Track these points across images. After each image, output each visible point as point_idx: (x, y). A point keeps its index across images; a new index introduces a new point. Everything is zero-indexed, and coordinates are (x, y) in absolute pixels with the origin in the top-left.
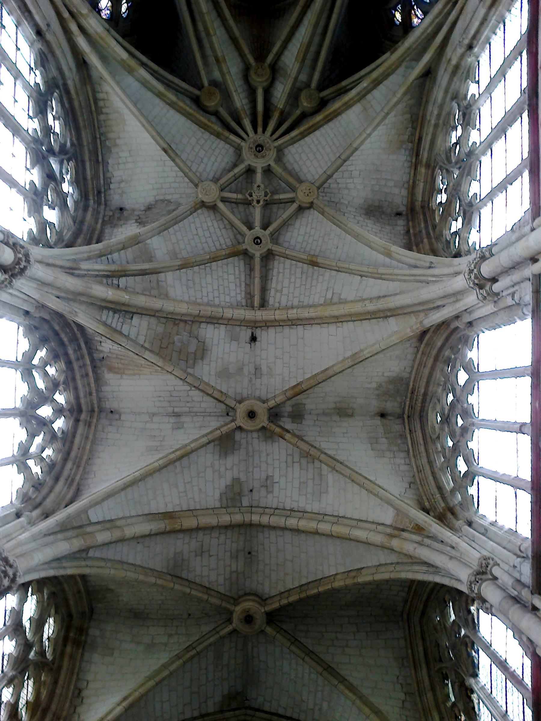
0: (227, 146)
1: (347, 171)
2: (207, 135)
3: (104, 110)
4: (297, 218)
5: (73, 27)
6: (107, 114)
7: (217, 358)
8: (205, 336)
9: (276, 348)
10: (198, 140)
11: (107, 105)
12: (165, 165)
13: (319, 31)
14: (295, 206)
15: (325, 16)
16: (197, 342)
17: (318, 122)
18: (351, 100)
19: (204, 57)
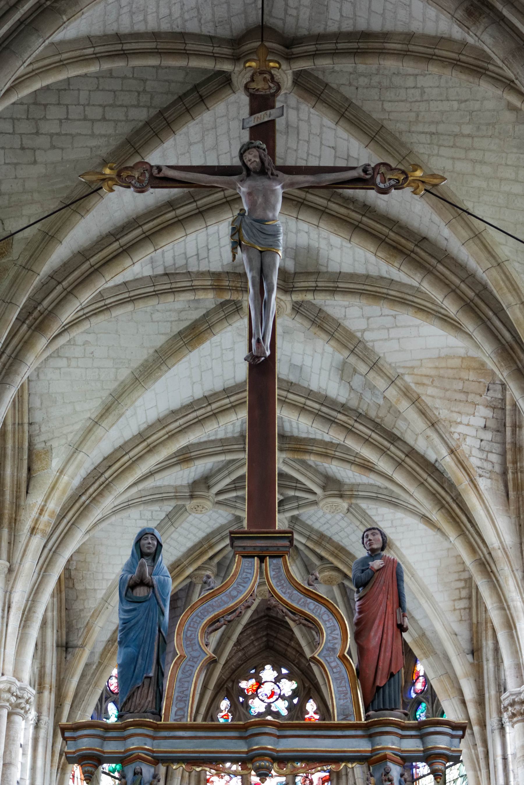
0: (309, 522)
1: (147, 520)
2: (336, 538)
3: (462, 584)
4: (211, 470)
6: (460, 580)
7: (322, 354)
8: (339, 386)
9: (233, 359)
10: (348, 536)
11: (457, 591)
12: (392, 521)
14: (215, 490)
16: (351, 383)
17: (191, 564)
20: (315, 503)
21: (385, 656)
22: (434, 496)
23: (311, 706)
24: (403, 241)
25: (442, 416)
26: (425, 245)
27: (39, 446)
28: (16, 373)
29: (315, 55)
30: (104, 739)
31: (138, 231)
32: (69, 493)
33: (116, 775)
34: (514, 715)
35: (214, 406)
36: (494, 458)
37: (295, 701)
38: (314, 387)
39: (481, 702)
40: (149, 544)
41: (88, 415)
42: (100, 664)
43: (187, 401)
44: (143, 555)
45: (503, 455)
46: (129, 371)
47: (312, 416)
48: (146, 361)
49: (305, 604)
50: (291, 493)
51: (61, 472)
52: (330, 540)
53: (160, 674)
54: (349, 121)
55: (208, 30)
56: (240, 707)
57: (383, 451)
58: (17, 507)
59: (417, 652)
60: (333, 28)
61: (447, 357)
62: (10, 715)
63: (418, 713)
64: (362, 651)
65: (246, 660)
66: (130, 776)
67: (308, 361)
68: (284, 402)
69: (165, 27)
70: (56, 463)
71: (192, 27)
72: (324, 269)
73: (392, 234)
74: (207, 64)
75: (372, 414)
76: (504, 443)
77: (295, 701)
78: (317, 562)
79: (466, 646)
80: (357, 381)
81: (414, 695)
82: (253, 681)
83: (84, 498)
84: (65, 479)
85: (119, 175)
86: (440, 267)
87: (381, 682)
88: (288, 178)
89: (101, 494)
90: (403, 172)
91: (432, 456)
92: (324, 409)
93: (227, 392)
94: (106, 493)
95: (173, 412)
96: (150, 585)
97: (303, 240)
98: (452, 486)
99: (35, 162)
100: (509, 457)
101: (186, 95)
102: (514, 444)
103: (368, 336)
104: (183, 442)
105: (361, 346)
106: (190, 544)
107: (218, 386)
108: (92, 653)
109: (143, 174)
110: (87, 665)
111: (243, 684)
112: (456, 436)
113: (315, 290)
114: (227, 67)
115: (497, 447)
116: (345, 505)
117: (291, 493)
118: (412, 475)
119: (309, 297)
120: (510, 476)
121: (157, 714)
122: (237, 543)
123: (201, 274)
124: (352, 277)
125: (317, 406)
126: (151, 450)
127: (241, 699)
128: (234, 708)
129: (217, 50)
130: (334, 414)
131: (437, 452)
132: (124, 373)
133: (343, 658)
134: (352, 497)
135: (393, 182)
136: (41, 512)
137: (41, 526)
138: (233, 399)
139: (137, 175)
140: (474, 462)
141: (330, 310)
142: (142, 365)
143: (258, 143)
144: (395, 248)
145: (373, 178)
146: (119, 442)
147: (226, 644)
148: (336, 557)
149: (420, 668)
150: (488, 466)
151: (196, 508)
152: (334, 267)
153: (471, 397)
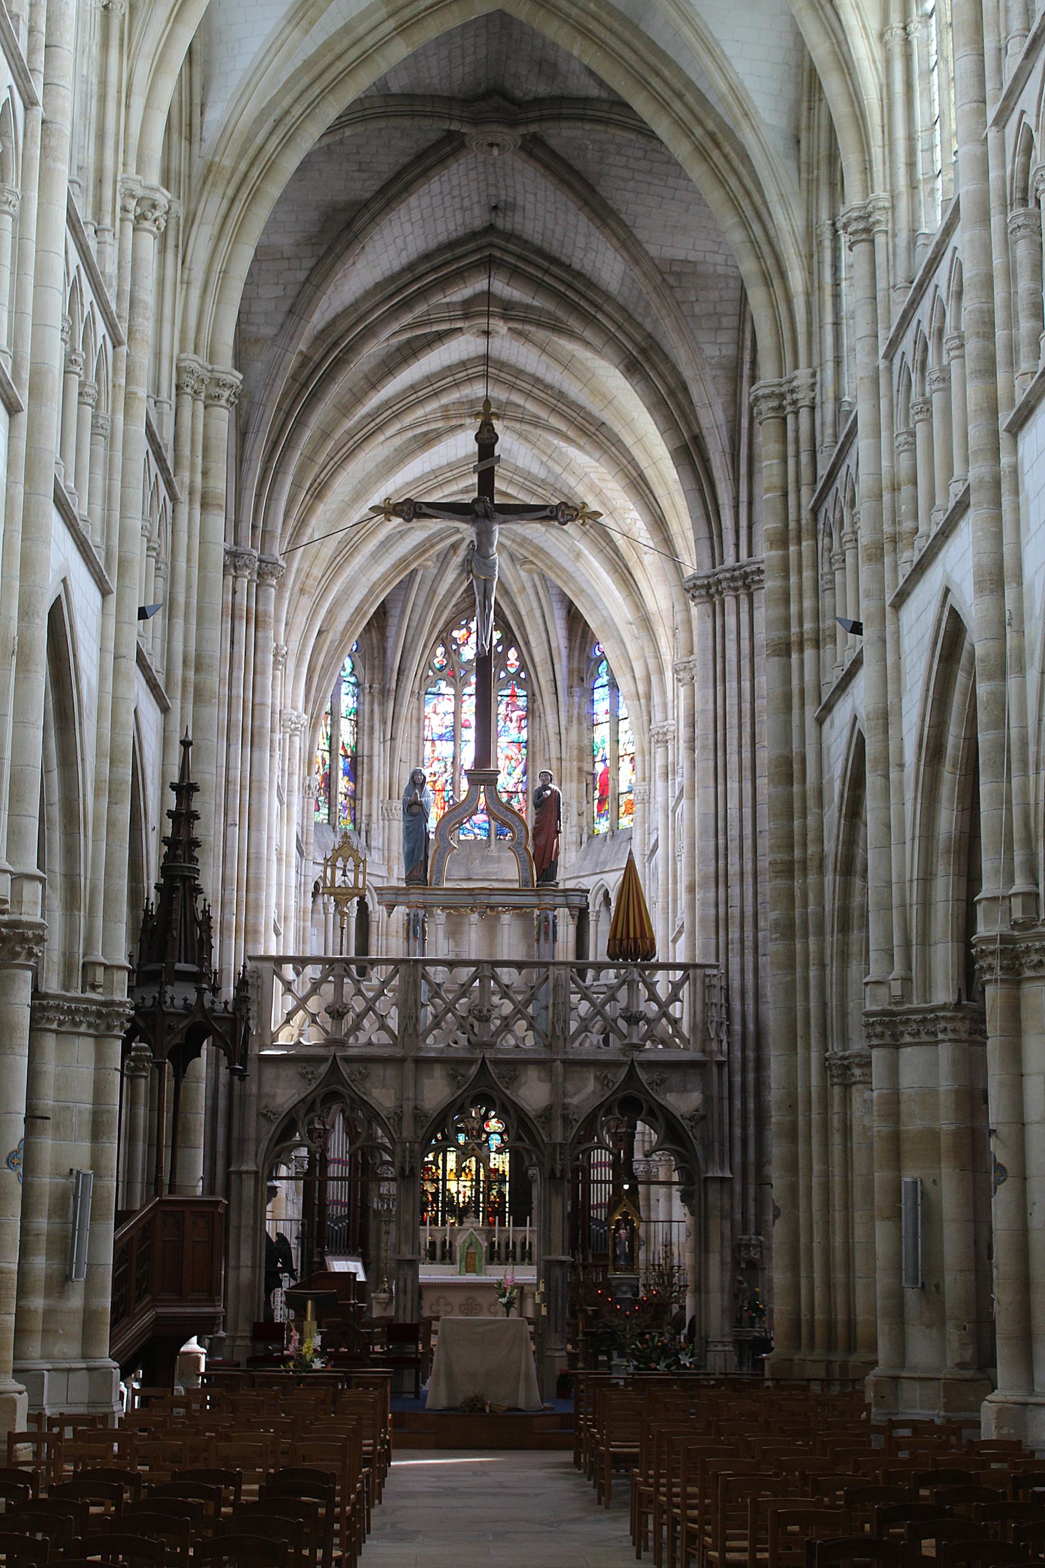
2: (535, 541)
13: (418, 610)
15: (414, 624)
17: (415, 559)
18: (383, 590)
19: (535, 586)
23: (512, 654)
24: (587, 425)
25: (618, 505)
26: (603, 429)
28: (304, 534)
33: (352, 717)
34: (658, 741)
35: (440, 478)
38: (520, 464)
41: (342, 498)
42: (341, 641)
43: (419, 475)
46: (373, 464)
47: (518, 488)
48: (388, 457)
49: (506, 816)
53: (426, 857)
56: (453, 654)
59: (599, 636)
63: (600, 669)
66: (412, 916)
73: (579, 419)
77: (500, 649)
81: (598, 653)
82: (464, 631)
83: (338, 559)
85: (394, 509)
86: (613, 449)
87: (545, 866)
89: (351, 555)
90: (576, 510)
92: (527, 483)
93: (451, 466)
94: (355, 554)
95: (407, 484)
105: (557, 451)
107: (444, 462)
109: (409, 508)
111: (456, 634)
112: (628, 521)
125: (522, 480)
127: (454, 647)
128: (447, 653)
130: (535, 487)
135: (569, 517)
138: (454, 472)
139: (405, 509)
142: (384, 460)
144: (581, 430)
145: (557, 515)
147: (442, 612)
148: (536, 556)
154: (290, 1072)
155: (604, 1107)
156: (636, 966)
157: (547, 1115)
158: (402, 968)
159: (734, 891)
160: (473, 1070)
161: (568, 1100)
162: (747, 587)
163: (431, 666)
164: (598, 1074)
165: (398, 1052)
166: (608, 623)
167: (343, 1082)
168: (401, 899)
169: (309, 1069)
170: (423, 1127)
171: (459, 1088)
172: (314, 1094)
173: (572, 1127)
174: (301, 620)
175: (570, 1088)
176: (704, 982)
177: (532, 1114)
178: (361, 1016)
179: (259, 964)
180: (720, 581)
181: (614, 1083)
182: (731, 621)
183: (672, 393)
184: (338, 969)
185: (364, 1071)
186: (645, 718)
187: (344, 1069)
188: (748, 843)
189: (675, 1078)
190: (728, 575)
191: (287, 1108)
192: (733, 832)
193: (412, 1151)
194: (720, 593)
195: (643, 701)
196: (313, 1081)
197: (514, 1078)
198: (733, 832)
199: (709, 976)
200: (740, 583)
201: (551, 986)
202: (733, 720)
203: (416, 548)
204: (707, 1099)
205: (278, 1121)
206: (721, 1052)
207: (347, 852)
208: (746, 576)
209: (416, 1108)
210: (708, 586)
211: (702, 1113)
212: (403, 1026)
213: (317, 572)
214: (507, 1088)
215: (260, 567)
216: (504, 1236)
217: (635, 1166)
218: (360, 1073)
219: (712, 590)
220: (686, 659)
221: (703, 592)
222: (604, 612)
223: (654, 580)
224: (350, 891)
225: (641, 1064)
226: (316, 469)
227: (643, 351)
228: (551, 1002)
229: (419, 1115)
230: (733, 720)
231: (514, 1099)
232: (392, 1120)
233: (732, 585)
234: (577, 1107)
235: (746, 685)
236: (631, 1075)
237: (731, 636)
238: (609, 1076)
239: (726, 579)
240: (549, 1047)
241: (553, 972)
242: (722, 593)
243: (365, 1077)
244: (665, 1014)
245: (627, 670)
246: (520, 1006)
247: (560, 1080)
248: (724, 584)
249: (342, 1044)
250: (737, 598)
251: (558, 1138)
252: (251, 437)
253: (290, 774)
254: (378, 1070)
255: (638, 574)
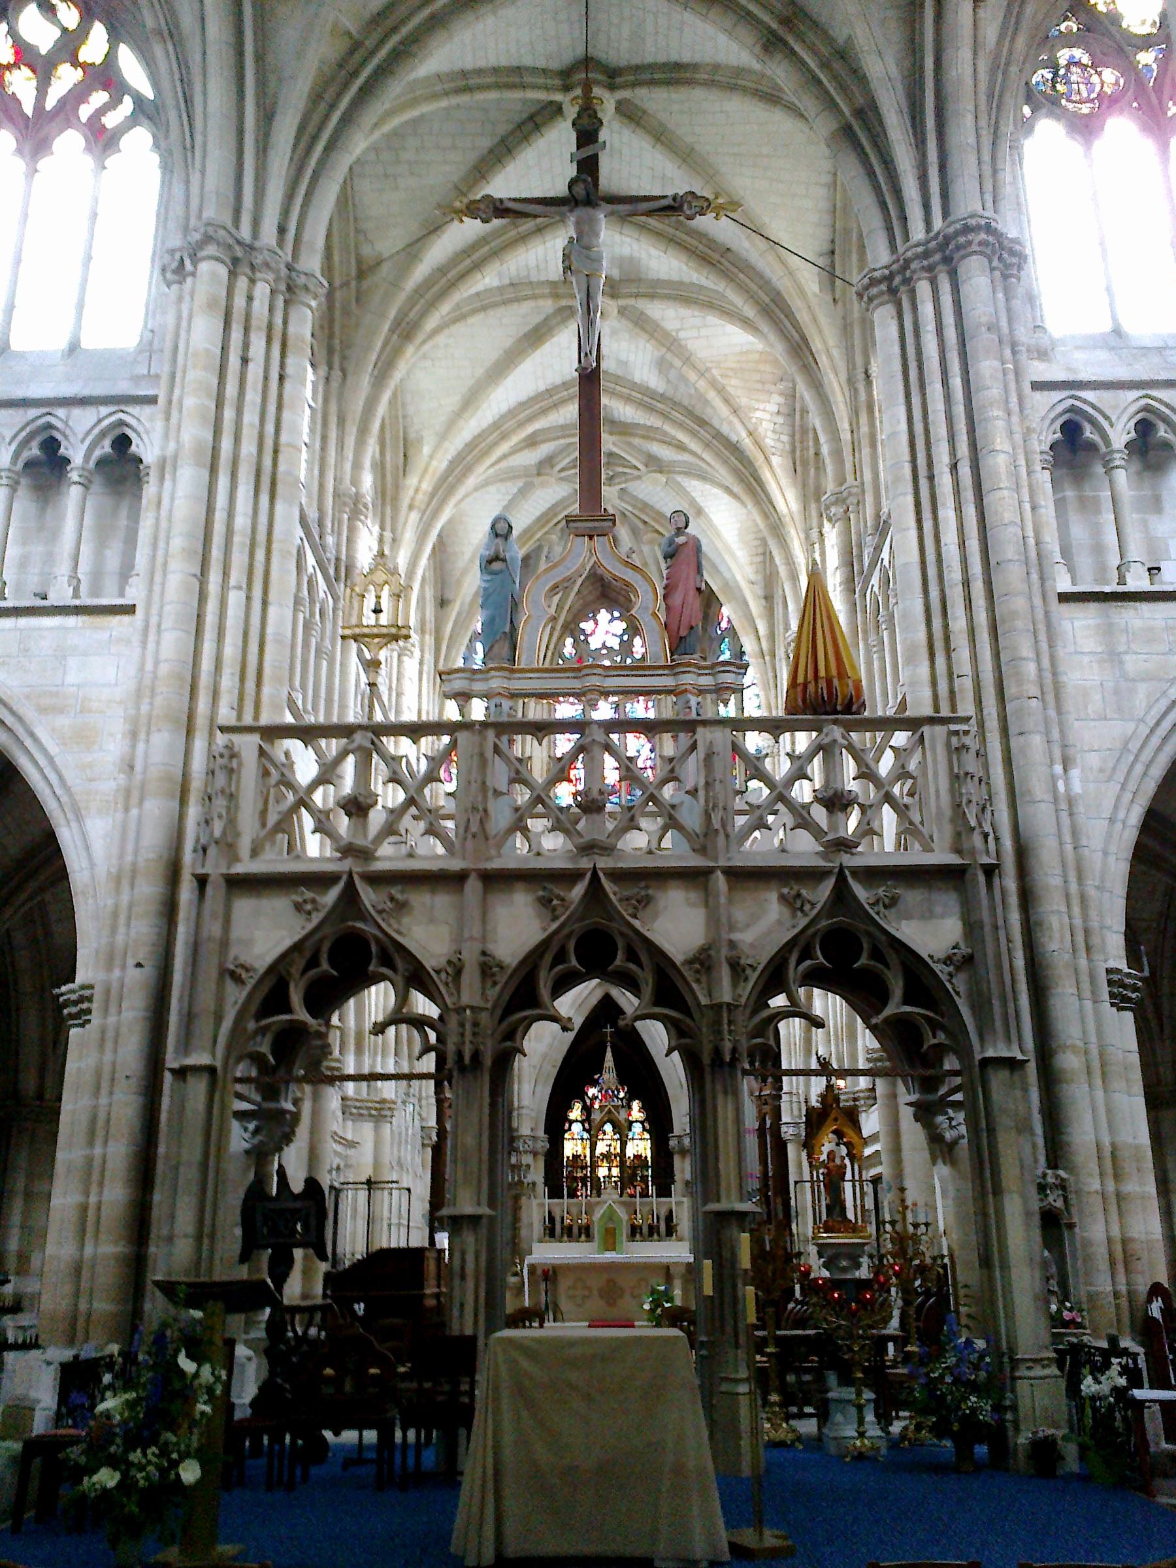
3: (757, 543)
5: (765, 645)
20: (639, 477)
21: (686, 612)
22: (736, 472)
23: (637, 641)
26: (729, 255)
27: (412, 435)
29: (634, 85)
30: (472, 680)
31: (486, 248)
32: (438, 475)
36: (785, 438)
37: (625, 638)
38: (637, 379)
39: (772, 636)
40: (502, 527)
42: (468, 612)
43: (532, 394)
44: (497, 535)
45: (793, 436)
50: (620, 469)
51: (431, 457)
52: (652, 507)
53: (514, 629)
54: (663, 144)
55: (541, 63)
57: (694, 434)
58: (397, 487)
60: (649, 59)
61: (748, 352)
62: (399, 656)
64: (668, 608)
65: (586, 605)
66: (493, 708)
67: (632, 358)
68: (613, 394)
69: (504, 62)
70: (426, 450)
71: (528, 61)
72: (643, 276)
73: (701, 247)
74: (542, 96)
75: (686, 402)
76: (793, 426)
78: (641, 525)
79: (760, 592)
80: (673, 374)
84: (434, 463)
86: (741, 276)
87: (683, 633)
88: (610, 207)
91: (734, 438)
96: (504, 560)
97: (626, 251)
98: (750, 463)
99: (397, 188)
100: (797, 437)
101: (524, 123)
102: (802, 427)
103: (682, 335)
104: (530, 429)
106: (538, 513)
107: (558, 381)
108: (462, 604)
110: (459, 614)
111: (583, 625)
113: (637, 296)
114: (558, 97)
115: (787, 429)
116: (663, 478)
117: (620, 469)
118: (718, 455)
119: (631, 302)
120: (798, 453)
121: (513, 660)
122: (572, 525)
123: (541, 284)
124: (668, 283)
126: (504, 437)
128: (575, 644)
129: (549, 81)
131: (738, 435)
132: (479, 372)
133: (654, 615)
134: (669, 472)
136: (417, 490)
137: (417, 503)
140: (769, 442)
141: (649, 312)
143: (584, 176)
145: (681, 206)
146: (477, 431)
149: (726, 611)
150: (779, 445)
151: (543, 485)
152: (653, 275)
153: (767, 387)
154: (279, 905)
155: (799, 945)
156: (835, 722)
157: (703, 961)
158: (462, 736)
159: (963, 655)
160: (578, 891)
161: (735, 936)
162: (947, 260)
163: (562, 656)
164: (785, 891)
165: (456, 865)
166: (728, 586)
167: (363, 915)
168: (478, 687)
169: (309, 895)
170: (495, 984)
171: (555, 919)
172: (317, 937)
173: (746, 979)
174: (409, 536)
175: (740, 914)
176: (948, 744)
177: (678, 958)
178: (396, 814)
179: (237, 739)
180: (908, 262)
181: (813, 905)
182: (927, 310)
183: (825, 65)
184: (360, 738)
185: (399, 896)
186: (771, 675)
187: (368, 896)
188: (978, 587)
189: (912, 897)
190: (920, 249)
191: (269, 959)
192: (954, 575)
193: (476, 1024)
194: (907, 281)
195: (767, 658)
196: (314, 915)
197: (645, 901)
198: (954, 575)
199: (957, 733)
200: (937, 257)
201: (702, 756)
202: (940, 430)
203: (539, 519)
204: (971, 928)
205: (253, 981)
206: (987, 852)
207: (380, 577)
208: (947, 239)
209: (484, 953)
210: (889, 278)
211: (965, 950)
212: (465, 828)
213: (426, 486)
214: (635, 916)
215: (290, 277)
216: (647, 1208)
217: (784, 1129)
218: (392, 899)
219: (897, 280)
220: (838, 490)
221: (883, 287)
222: (727, 575)
223: (785, 481)
224: (384, 631)
225: (857, 872)
226: (401, 298)
227: (786, 21)
228: (702, 782)
229: (488, 968)
230: (940, 430)
231: (647, 934)
232: (443, 975)
233: (925, 263)
234: (752, 945)
235: (956, 382)
236: (841, 893)
237: (928, 328)
238: (804, 892)
239: (917, 257)
240: (702, 850)
241: (702, 734)
242: (911, 279)
243: (401, 907)
244: (888, 798)
245: (750, 630)
246: (651, 789)
247: (723, 900)
248: (914, 265)
249: (365, 854)
250: (933, 282)
251: (727, 997)
252: (277, 125)
253: (399, 695)
254: (420, 899)
255: (766, 475)
